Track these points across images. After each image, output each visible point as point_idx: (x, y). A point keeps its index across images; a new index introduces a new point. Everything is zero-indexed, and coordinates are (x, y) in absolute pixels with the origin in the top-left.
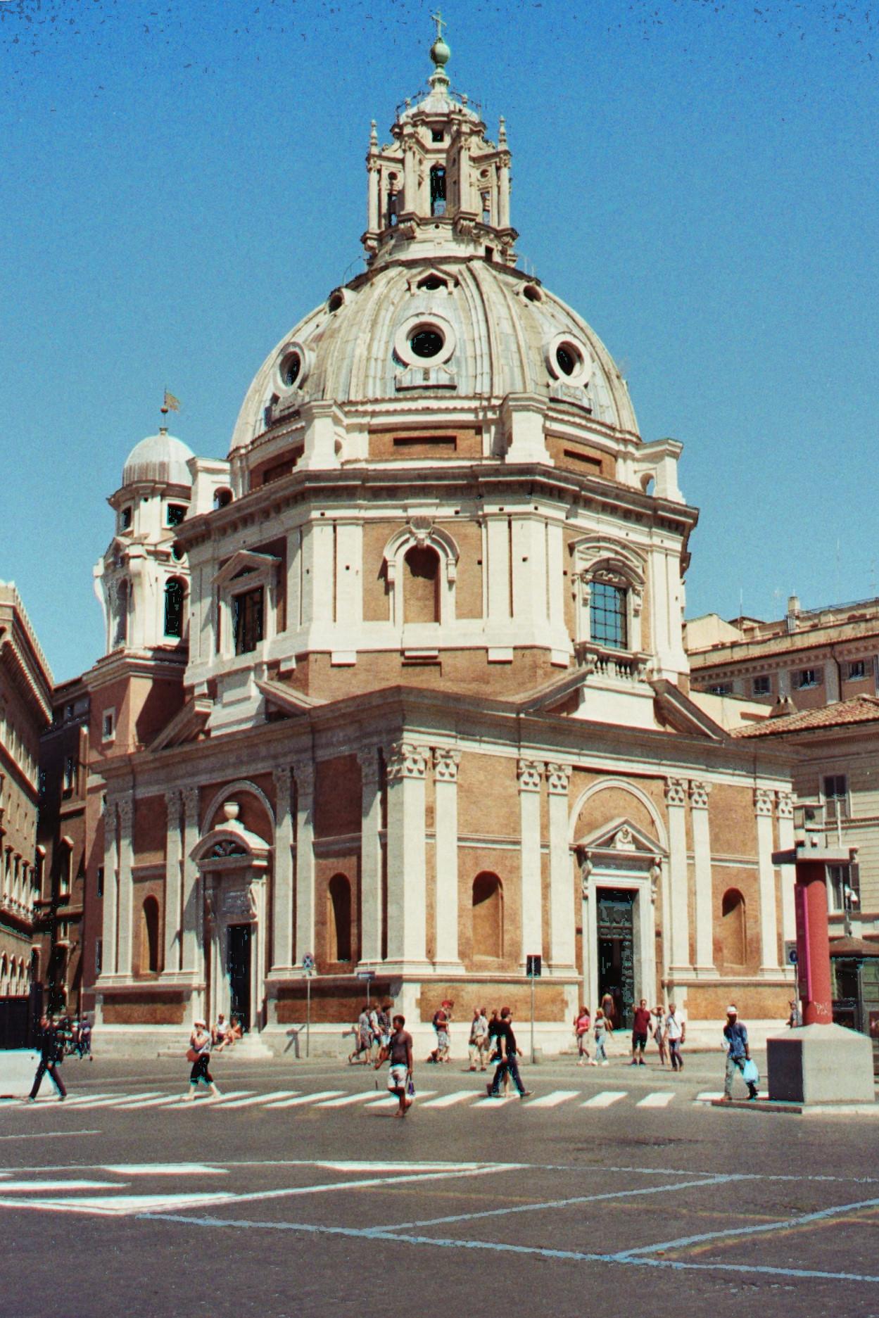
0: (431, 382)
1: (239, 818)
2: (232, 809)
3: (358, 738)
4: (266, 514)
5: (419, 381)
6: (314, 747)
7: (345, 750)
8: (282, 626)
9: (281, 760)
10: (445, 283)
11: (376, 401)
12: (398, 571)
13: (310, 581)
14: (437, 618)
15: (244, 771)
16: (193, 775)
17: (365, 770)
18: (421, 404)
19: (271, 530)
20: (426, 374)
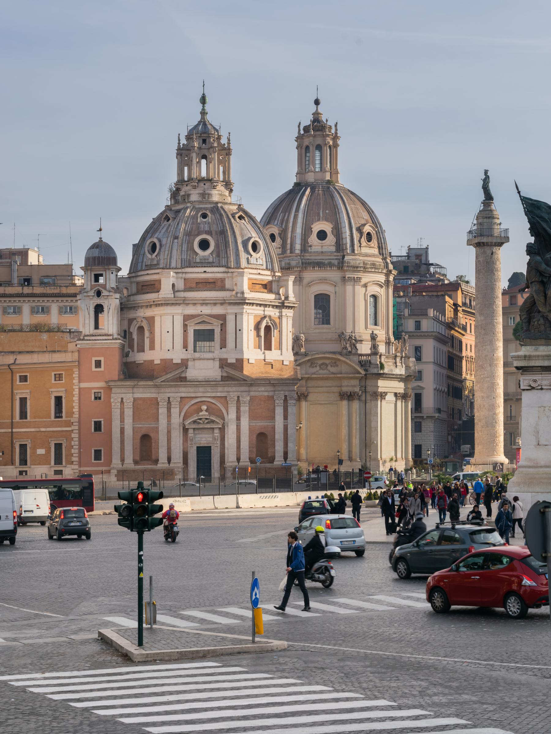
0: (258, 263)
1: (206, 411)
2: (204, 407)
3: (274, 391)
4: (215, 304)
5: (255, 262)
6: (249, 391)
7: (266, 394)
8: (223, 345)
9: (231, 393)
10: (243, 218)
11: (246, 268)
12: (262, 333)
13: (242, 333)
14: (270, 349)
15: (209, 395)
16: (177, 393)
17: (277, 401)
18: (259, 271)
19: (218, 310)
20: (257, 259)
